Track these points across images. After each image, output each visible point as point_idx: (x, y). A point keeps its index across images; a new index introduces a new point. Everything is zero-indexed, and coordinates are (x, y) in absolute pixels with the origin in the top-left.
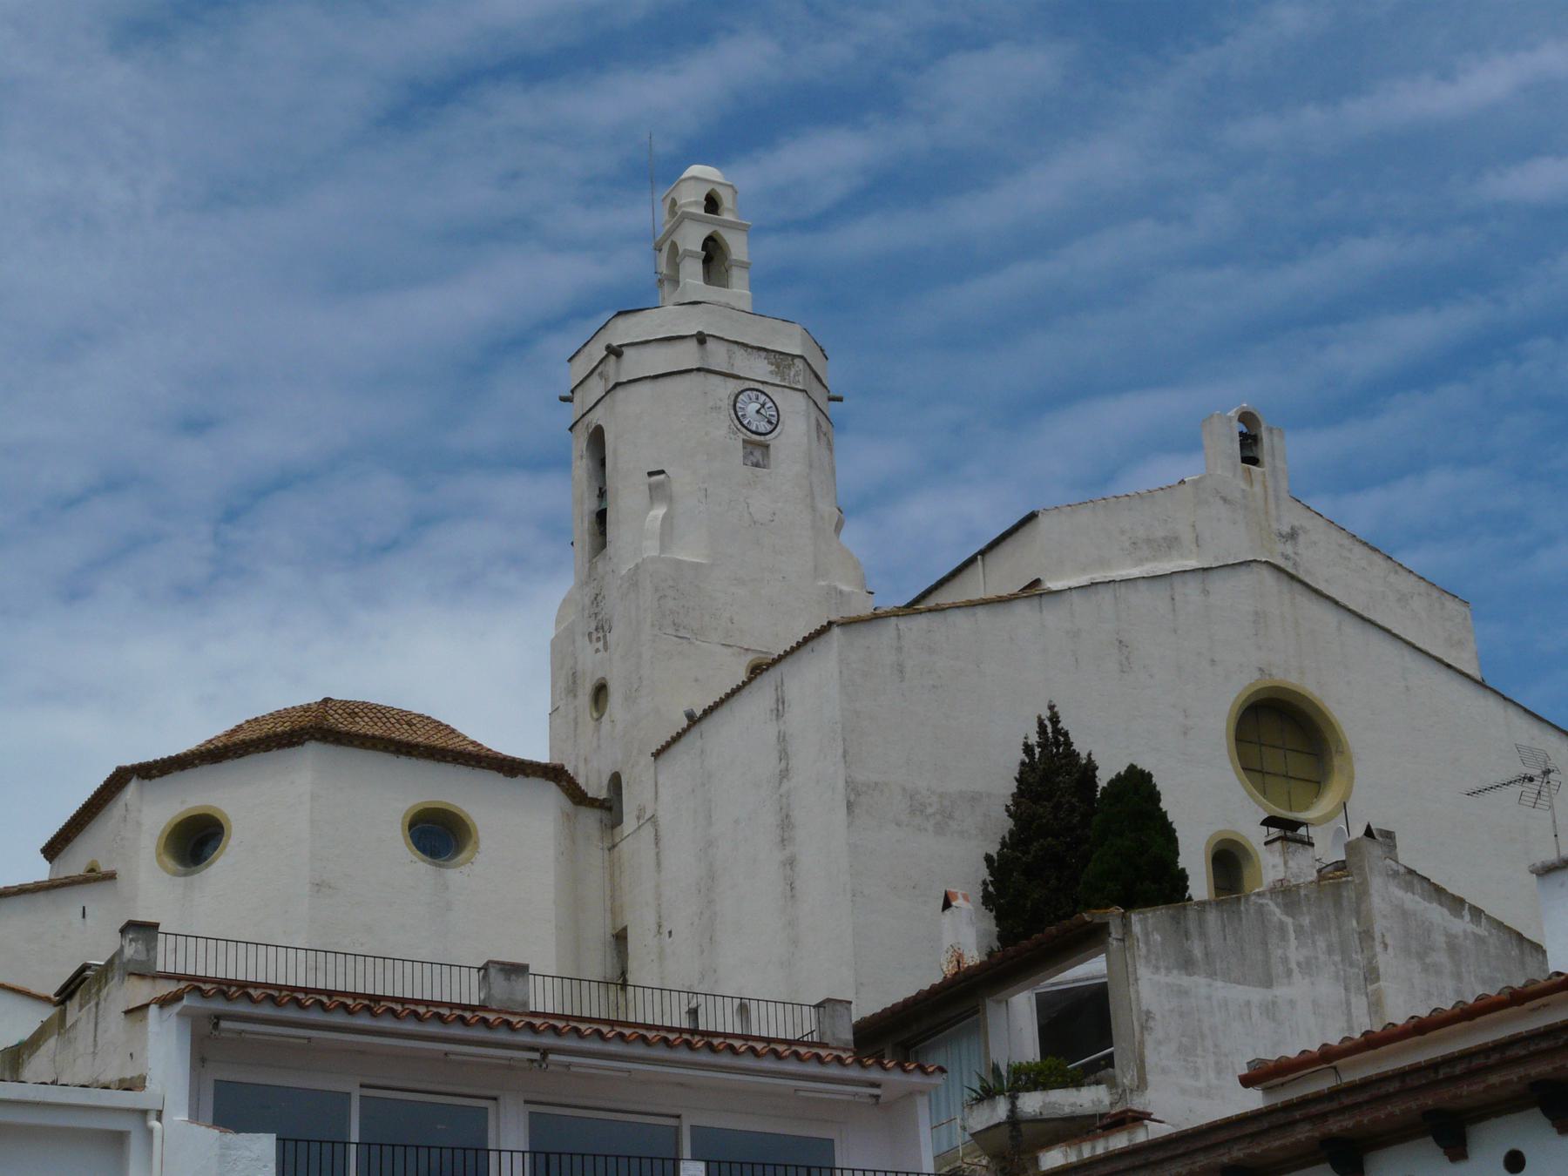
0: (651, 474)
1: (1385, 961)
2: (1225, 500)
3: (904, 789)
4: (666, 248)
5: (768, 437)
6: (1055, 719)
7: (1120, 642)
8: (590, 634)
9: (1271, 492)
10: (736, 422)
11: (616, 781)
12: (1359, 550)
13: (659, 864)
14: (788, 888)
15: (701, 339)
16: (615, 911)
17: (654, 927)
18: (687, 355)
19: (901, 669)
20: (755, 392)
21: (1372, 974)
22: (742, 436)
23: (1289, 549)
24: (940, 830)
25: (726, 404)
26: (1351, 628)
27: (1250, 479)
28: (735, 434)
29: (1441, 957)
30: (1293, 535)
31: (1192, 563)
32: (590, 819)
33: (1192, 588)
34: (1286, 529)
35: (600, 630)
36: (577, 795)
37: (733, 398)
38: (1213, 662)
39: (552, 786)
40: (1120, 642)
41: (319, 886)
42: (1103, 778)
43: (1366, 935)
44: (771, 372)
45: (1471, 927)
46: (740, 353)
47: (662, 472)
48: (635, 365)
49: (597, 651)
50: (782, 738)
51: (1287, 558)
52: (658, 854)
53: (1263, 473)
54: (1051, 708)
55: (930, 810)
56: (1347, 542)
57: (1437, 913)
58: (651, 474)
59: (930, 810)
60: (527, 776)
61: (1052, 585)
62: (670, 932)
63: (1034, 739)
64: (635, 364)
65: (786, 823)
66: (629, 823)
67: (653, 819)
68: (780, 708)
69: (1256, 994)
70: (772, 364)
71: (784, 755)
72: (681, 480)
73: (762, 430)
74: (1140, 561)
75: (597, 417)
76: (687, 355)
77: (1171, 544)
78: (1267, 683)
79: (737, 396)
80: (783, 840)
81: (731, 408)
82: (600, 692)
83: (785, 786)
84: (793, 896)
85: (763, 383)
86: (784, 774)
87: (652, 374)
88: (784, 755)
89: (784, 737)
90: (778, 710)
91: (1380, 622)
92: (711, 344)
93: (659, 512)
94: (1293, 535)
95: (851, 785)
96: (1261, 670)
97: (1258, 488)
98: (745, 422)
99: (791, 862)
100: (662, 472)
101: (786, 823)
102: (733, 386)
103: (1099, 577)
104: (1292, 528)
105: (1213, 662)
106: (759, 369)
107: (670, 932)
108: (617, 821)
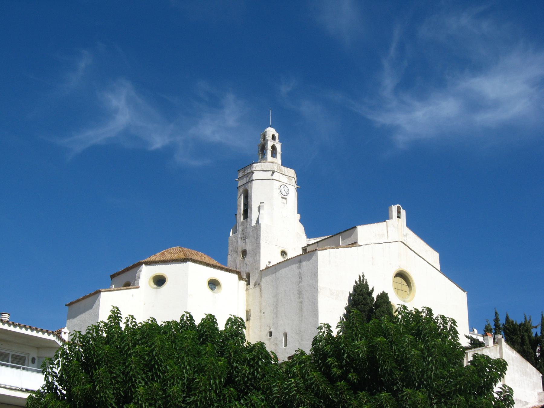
0: (261, 203)
2: (394, 226)
3: (330, 289)
5: (287, 196)
6: (363, 276)
7: (373, 258)
8: (241, 238)
9: (402, 225)
10: (280, 192)
13: (261, 296)
14: (300, 308)
17: (259, 311)
20: (284, 186)
22: (281, 196)
23: (405, 238)
25: (278, 188)
28: (280, 195)
30: (406, 235)
34: (405, 234)
36: (240, 278)
37: (280, 186)
38: (390, 264)
39: (237, 276)
40: (373, 258)
44: (288, 181)
45: (515, 356)
47: (263, 203)
49: (244, 242)
50: (300, 273)
51: (405, 240)
52: (261, 294)
53: (401, 220)
54: (363, 273)
55: (334, 294)
58: (261, 203)
59: (334, 294)
60: (232, 273)
62: (264, 313)
63: (358, 280)
65: (300, 293)
68: (300, 267)
70: (288, 179)
71: (300, 277)
73: (286, 195)
79: (281, 186)
80: (299, 297)
81: (279, 189)
83: (301, 284)
84: (301, 310)
85: (286, 183)
87: (261, 179)
88: (300, 277)
89: (301, 273)
90: (299, 267)
91: (422, 257)
94: (406, 235)
96: (399, 266)
97: (400, 224)
98: (282, 193)
99: (301, 302)
100: (263, 203)
104: (406, 234)
105: (390, 264)
106: (284, 179)
107: (264, 313)
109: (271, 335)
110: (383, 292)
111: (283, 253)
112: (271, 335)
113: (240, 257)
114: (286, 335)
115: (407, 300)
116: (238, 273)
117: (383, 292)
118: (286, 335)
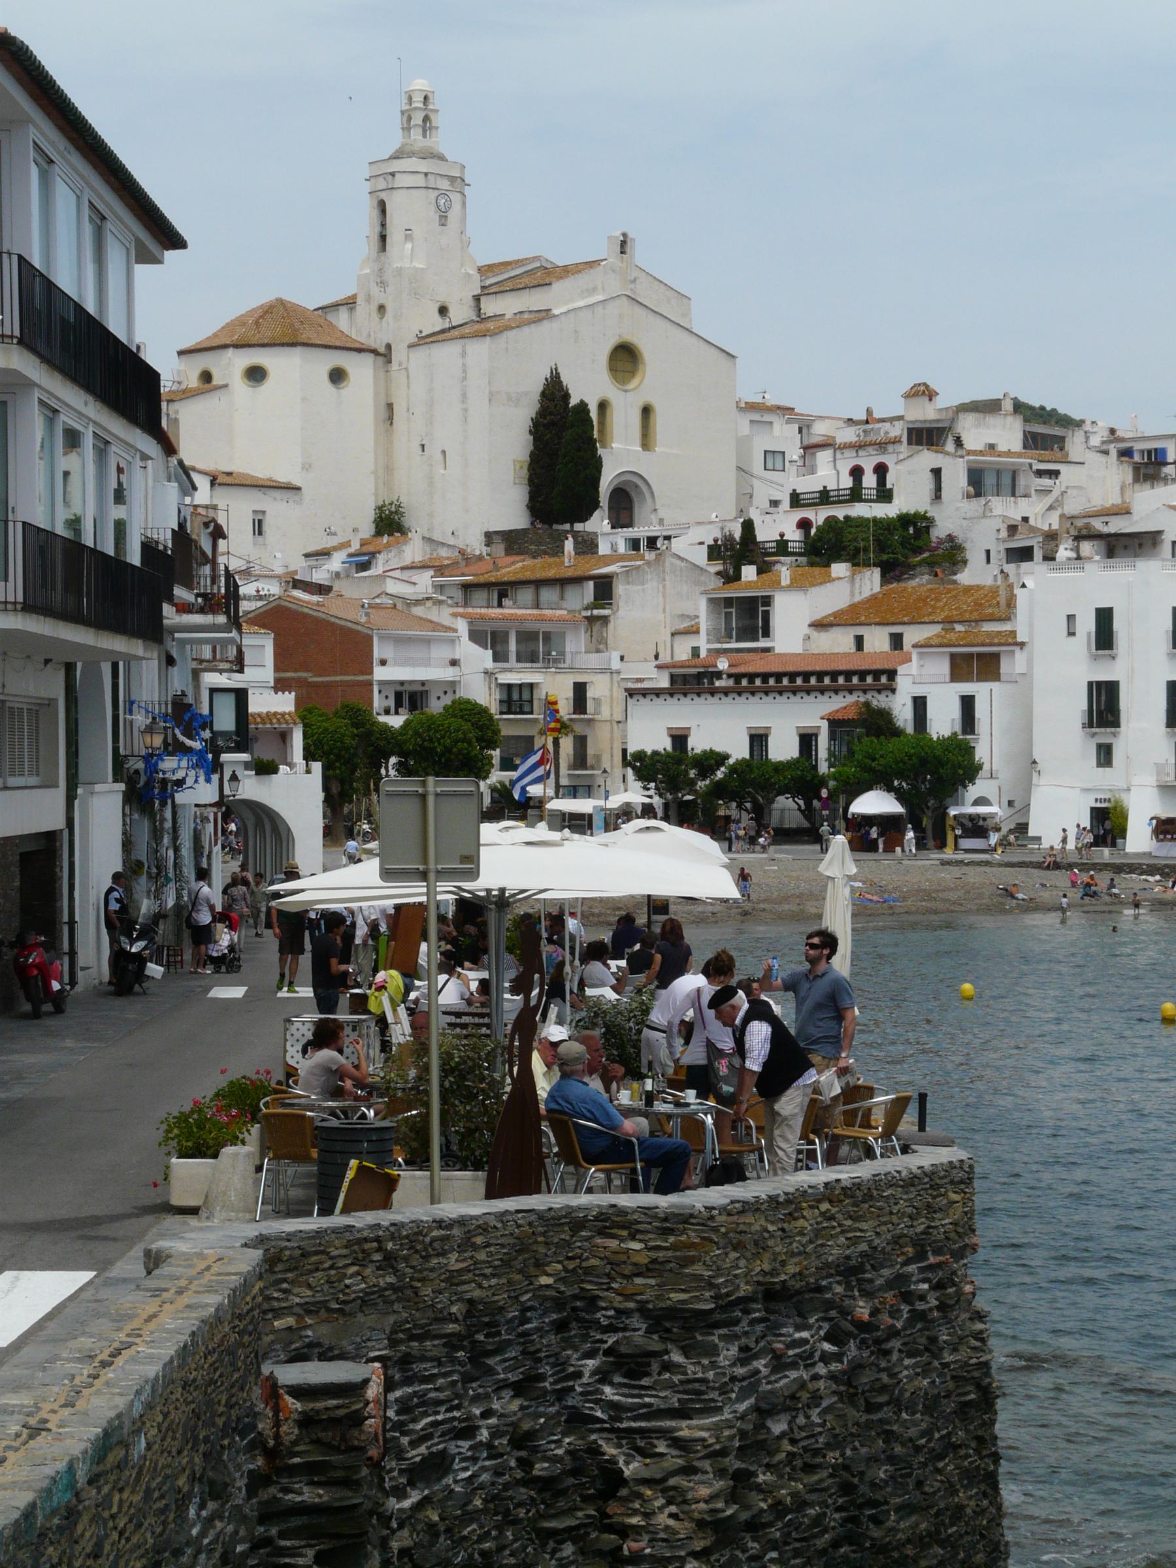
1: (667, 577)
4: (406, 115)
11: (389, 347)
12: (657, 283)
15: (426, 174)
16: (388, 395)
18: (420, 181)
19: (507, 349)
21: (664, 580)
23: (632, 286)
24: (516, 406)
26: (651, 316)
27: (622, 261)
29: (678, 573)
30: (634, 281)
31: (601, 298)
32: (380, 359)
33: (599, 310)
35: (383, 284)
41: (304, 399)
42: (573, 402)
43: (664, 571)
46: (439, 178)
48: (401, 180)
50: (464, 365)
56: (652, 280)
57: (678, 562)
61: (556, 312)
64: (401, 180)
65: (464, 396)
66: (394, 366)
67: (406, 369)
69: (640, 587)
71: (465, 371)
72: (417, 233)
74: (583, 298)
75: (383, 195)
76: (420, 181)
77: (594, 290)
78: (621, 340)
82: (382, 308)
86: (464, 378)
88: (465, 371)
92: (429, 176)
93: (409, 246)
94: (634, 281)
95: (491, 394)
99: (466, 410)
101: (464, 396)
102: (437, 193)
103: (570, 307)
106: (444, 184)
108: (390, 362)
109: (423, 451)
110: (582, 401)
111: (443, 311)
112: (423, 451)
113: (375, 315)
114: (444, 452)
115: (630, 386)
116: (375, 352)
117: (582, 401)
118: (444, 452)
